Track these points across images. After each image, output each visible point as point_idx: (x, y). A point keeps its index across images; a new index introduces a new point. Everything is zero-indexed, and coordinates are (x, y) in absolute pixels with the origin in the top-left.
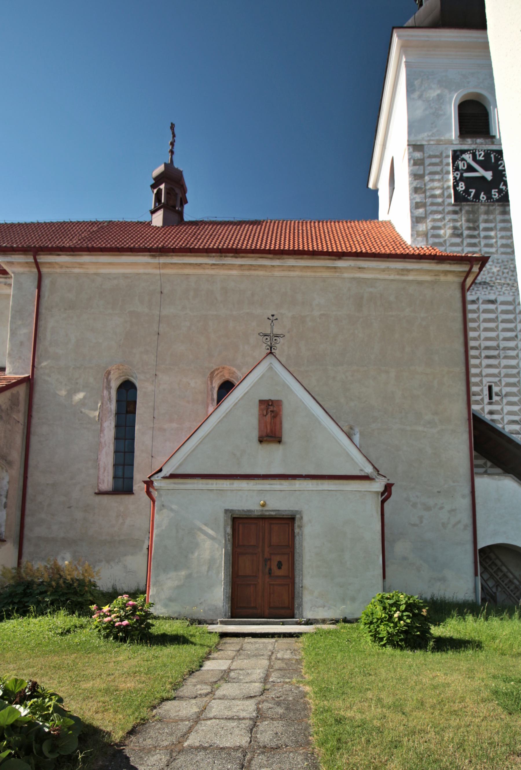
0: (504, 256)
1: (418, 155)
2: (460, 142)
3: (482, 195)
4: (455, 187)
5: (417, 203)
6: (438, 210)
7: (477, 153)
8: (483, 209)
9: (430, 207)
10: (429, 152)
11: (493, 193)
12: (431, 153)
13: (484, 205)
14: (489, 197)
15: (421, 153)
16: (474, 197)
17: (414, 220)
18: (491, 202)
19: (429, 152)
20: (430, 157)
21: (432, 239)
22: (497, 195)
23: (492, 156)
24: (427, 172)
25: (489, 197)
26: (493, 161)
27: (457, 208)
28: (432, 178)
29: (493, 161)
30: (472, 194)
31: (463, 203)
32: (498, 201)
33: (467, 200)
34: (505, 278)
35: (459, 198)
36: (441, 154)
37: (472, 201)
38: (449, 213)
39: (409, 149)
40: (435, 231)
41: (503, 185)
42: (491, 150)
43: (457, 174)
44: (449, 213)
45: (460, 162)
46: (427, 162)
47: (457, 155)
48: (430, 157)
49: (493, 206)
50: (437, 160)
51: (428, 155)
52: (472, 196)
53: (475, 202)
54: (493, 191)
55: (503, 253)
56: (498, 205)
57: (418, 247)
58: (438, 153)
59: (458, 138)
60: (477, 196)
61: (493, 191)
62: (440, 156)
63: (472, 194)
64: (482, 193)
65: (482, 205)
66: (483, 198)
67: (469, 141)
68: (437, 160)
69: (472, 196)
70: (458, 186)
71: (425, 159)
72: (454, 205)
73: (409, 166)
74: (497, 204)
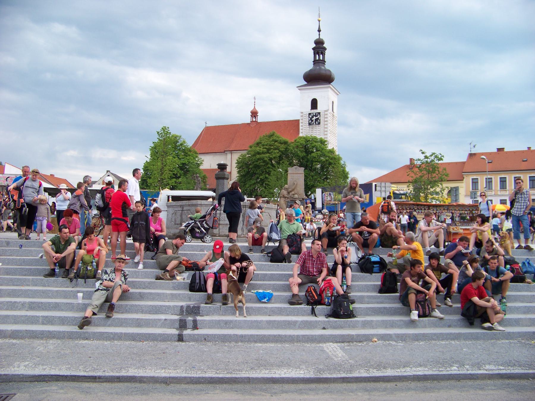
4: (309, 121)
8: (314, 126)
10: (304, 113)
19: (304, 113)
33: (311, 125)
38: (308, 127)
44: (308, 127)
47: (310, 114)
67: (312, 110)
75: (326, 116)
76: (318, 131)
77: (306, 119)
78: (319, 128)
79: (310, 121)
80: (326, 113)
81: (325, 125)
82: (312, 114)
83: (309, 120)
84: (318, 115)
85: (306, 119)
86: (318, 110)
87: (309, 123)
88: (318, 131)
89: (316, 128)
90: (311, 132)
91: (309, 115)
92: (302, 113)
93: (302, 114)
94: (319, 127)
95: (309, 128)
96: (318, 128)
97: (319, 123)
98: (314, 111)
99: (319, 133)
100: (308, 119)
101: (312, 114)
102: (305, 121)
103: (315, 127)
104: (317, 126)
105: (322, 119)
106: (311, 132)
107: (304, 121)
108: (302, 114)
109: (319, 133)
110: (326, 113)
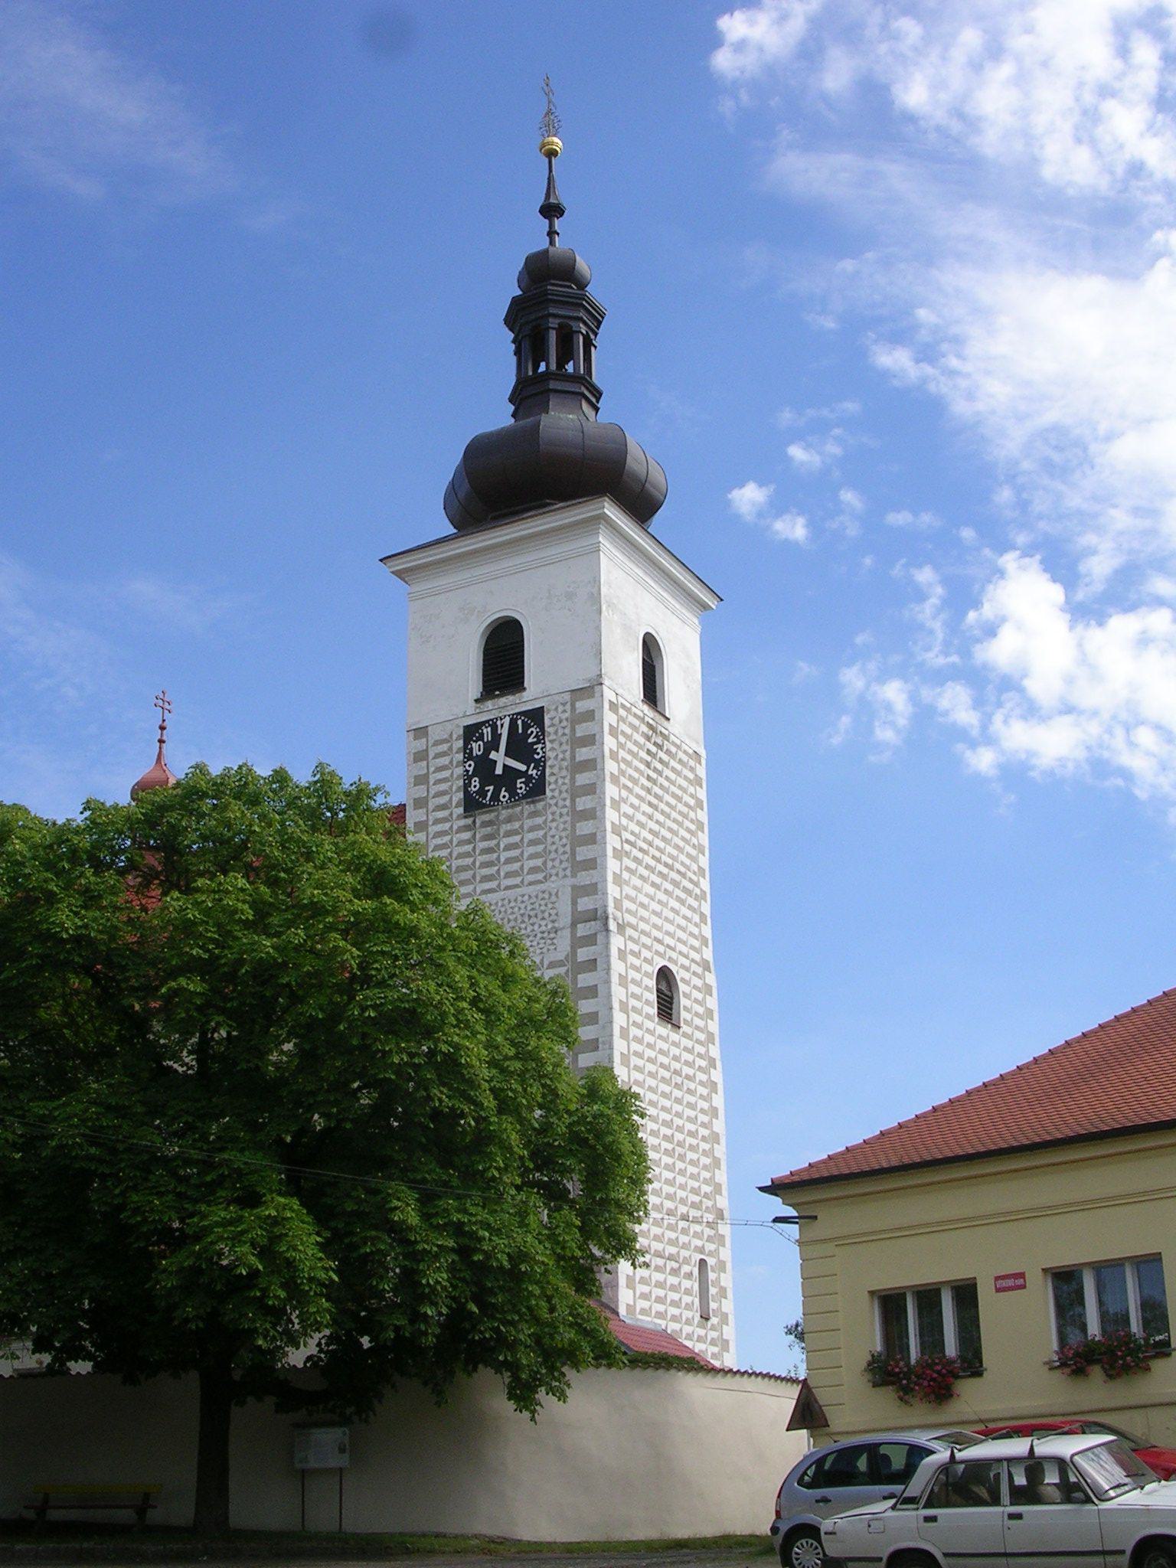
0: (531, 888)
3: (503, 793)
4: (466, 786)
7: (499, 723)
8: (505, 813)
10: (435, 734)
11: (518, 786)
12: (438, 738)
13: (508, 808)
14: (513, 792)
16: (490, 801)
18: (515, 800)
19: (435, 734)
20: (437, 743)
22: (523, 786)
23: (519, 722)
25: (513, 792)
26: (520, 731)
27: (469, 821)
29: (520, 731)
30: (489, 794)
31: (476, 812)
32: (524, 797)
33: (485, 806)
34: (533, 925)
35: (472, 804)
37: (490, 806)
38: (460, 830)
41: (534, 768)
42: (517, 714)
44: (460, 830)
45: (474, 744)
47: (471, 732)
48: (437, 743)
49: (519, 805)
50: (445, 747)
52: (488, 798)
53: (494, 805)
54: (519, 781)
55: (530, 884)
56: (527, 803)
58: (446, 736)
60: (495, 797)
61: (519, 781)
63: (489, 794)
64: (504, 789)
65: (504, 808)
66: (504, 797)
69: (488, 798)
71: (429, 749)
72: (466, 817)
74: (524, 801)
75: (581, 730)
76: (532, 843)
77: (446, 774)
78: (539, 820)
79: (476, 782)
80: (582, 706)
81: (576, 792)
82: (487, 731)
83: (468, 778)
84: (526, 726)
85: (446, 774)
86: (526, 695)
87: (466, 793)
88: (532, 843)
89: (517, 825)
90: (481, 859)
91: (466, 743)
92: (421, 732)
93: (421, 744)
94: (534, 814)
95: (466, 835)
96: (528, 823)
97: (537, 789)
98: (507, 706)
99: (539, 862)
100: (460, 771)
101: (487, 731)
102: (443, 787)
103: (509, 820)
104: (528, 808)
105: (554, 751)
106: (481, 859)
107: (433, 790)
108: (421, 744)
109: (539, 862)
110: (582, 706)
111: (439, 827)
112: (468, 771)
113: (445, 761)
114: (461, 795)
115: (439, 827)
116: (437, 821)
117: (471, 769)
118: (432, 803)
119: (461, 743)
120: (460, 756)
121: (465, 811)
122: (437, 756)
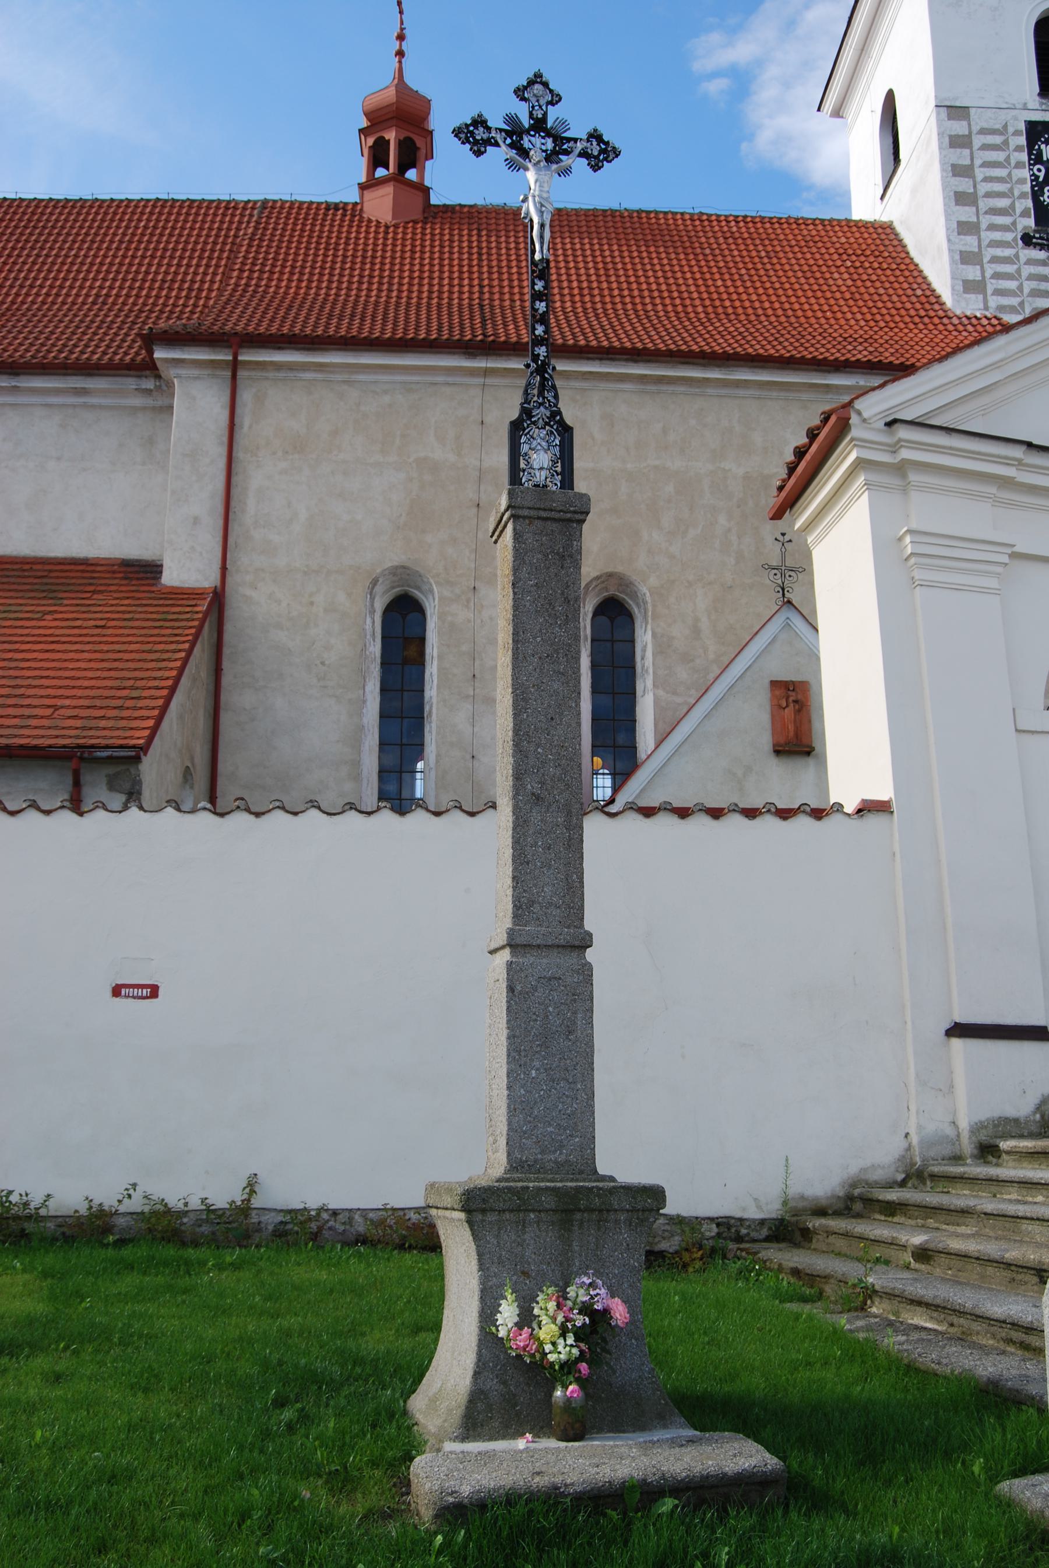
1: (959, 128)
2: (1041, 104)
5: (960, 224)
6: (1004, 239)
9: (988, 233)
10: (979, 120)
12: (985, 125)
15: (965, 123)
17: (957, 257)
19: (979, 120)
20: (983, 132)
21: (994, 297)
24: (978, 162)
28: (988, 175)
36: (1005, 127)
39: (938, 114)
40: (1000, 282)
43: (1039, 170)
46: (978, 141)
48: (983, 132)
50: (998, 140)
51: (978, 128)
57: (968, 313)
58: (998, 126)
59: (1037, 98)
62: (1003, 131)
68: (998, 140)
70: (1043, 194)
71: (973, 137)
73: (940, 148)
100: (1025, 173)
107: (983, 188)
111: (997, 236)
112: (1037, 177)
113: (999, 156)
114: (1029, 203)
115: (997, 236)
116: (992, 227)
117: (1042, 175)
118: (984, 204)
119: (1022, 140)
120: (1024, 157)
121: (1036, 225)
122: (985, 147)
